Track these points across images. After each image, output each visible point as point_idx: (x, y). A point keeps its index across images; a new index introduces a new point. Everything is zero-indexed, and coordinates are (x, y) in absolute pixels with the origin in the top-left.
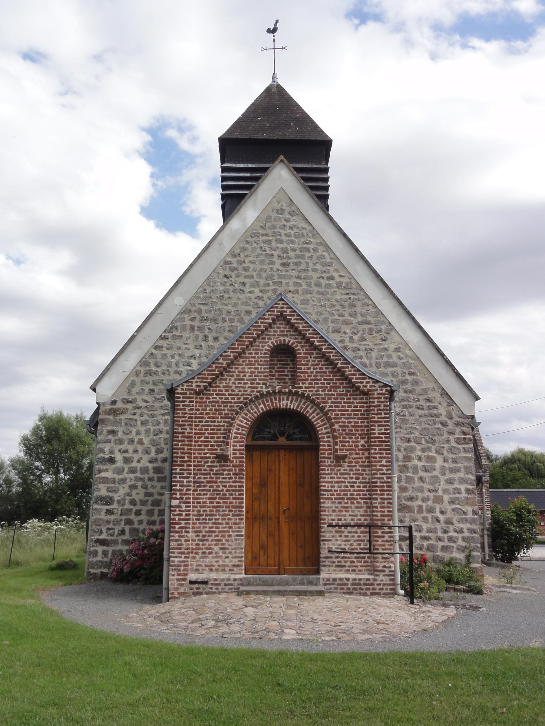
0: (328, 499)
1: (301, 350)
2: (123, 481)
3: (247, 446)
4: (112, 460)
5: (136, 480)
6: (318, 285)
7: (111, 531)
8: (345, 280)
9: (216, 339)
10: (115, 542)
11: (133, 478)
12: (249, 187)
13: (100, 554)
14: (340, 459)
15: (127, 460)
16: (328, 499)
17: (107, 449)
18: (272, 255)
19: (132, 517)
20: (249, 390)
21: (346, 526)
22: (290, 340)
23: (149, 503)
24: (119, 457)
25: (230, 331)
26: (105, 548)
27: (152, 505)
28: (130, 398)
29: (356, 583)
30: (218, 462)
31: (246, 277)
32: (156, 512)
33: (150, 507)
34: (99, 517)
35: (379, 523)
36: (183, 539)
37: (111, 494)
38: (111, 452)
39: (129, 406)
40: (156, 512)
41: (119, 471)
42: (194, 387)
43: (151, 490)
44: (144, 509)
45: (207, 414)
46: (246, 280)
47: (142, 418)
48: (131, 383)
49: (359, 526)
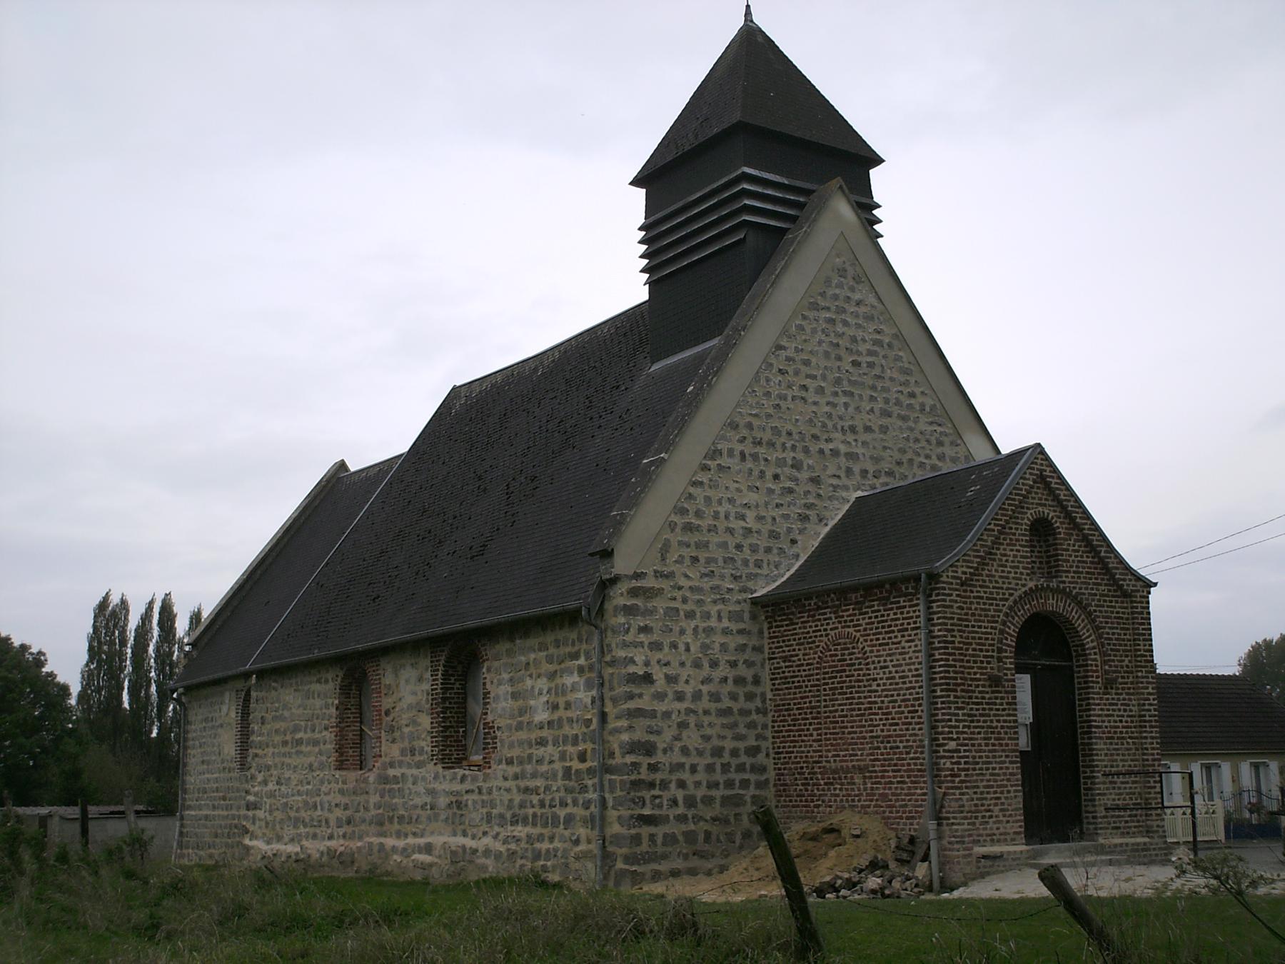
0: (1101, 738)
1: (1060, 525)
2: (667, 715)
3: (1016, 664)
4: (648, 679)
5: (687, 714)
6: (898, 403)
7: (657, 801)
8: (929, 402)
9: (776, 477)
10: (665, 820)
11: (683, 711)
12: (793, 219)
13: (645, 841)
14: (1109, 684)
15: (671, 679)
16: (1101, 738)
17: (639, 659)
18: (838, 345)
19: (686, 776)
20: (1014, 582)
21: (1118, 774)
22: (1051, 513)
23: (708, 752)
24: (658, 674)
25: (792, 466)
26: (652, 830)
27: (712, 755)
28: (666, 570)
29: (1136, 849)
30: (990, 686)
31: (808, 376)
32: (718, 767)
33: (709, 760)
34: (638, 777)
35: (1151, 769)
36: (965, 797)
37: (652, 738)
38: (647, 664)
39: (665, 584)
40: (718, 767)
41: (660, 696)
42: (959, 574)
43: (709, 731)
44: (702, 762)
45: (973, 615)
46: (808, 382)
47: (685, 607)
48: (664, 545)
49: (1129, 773)
